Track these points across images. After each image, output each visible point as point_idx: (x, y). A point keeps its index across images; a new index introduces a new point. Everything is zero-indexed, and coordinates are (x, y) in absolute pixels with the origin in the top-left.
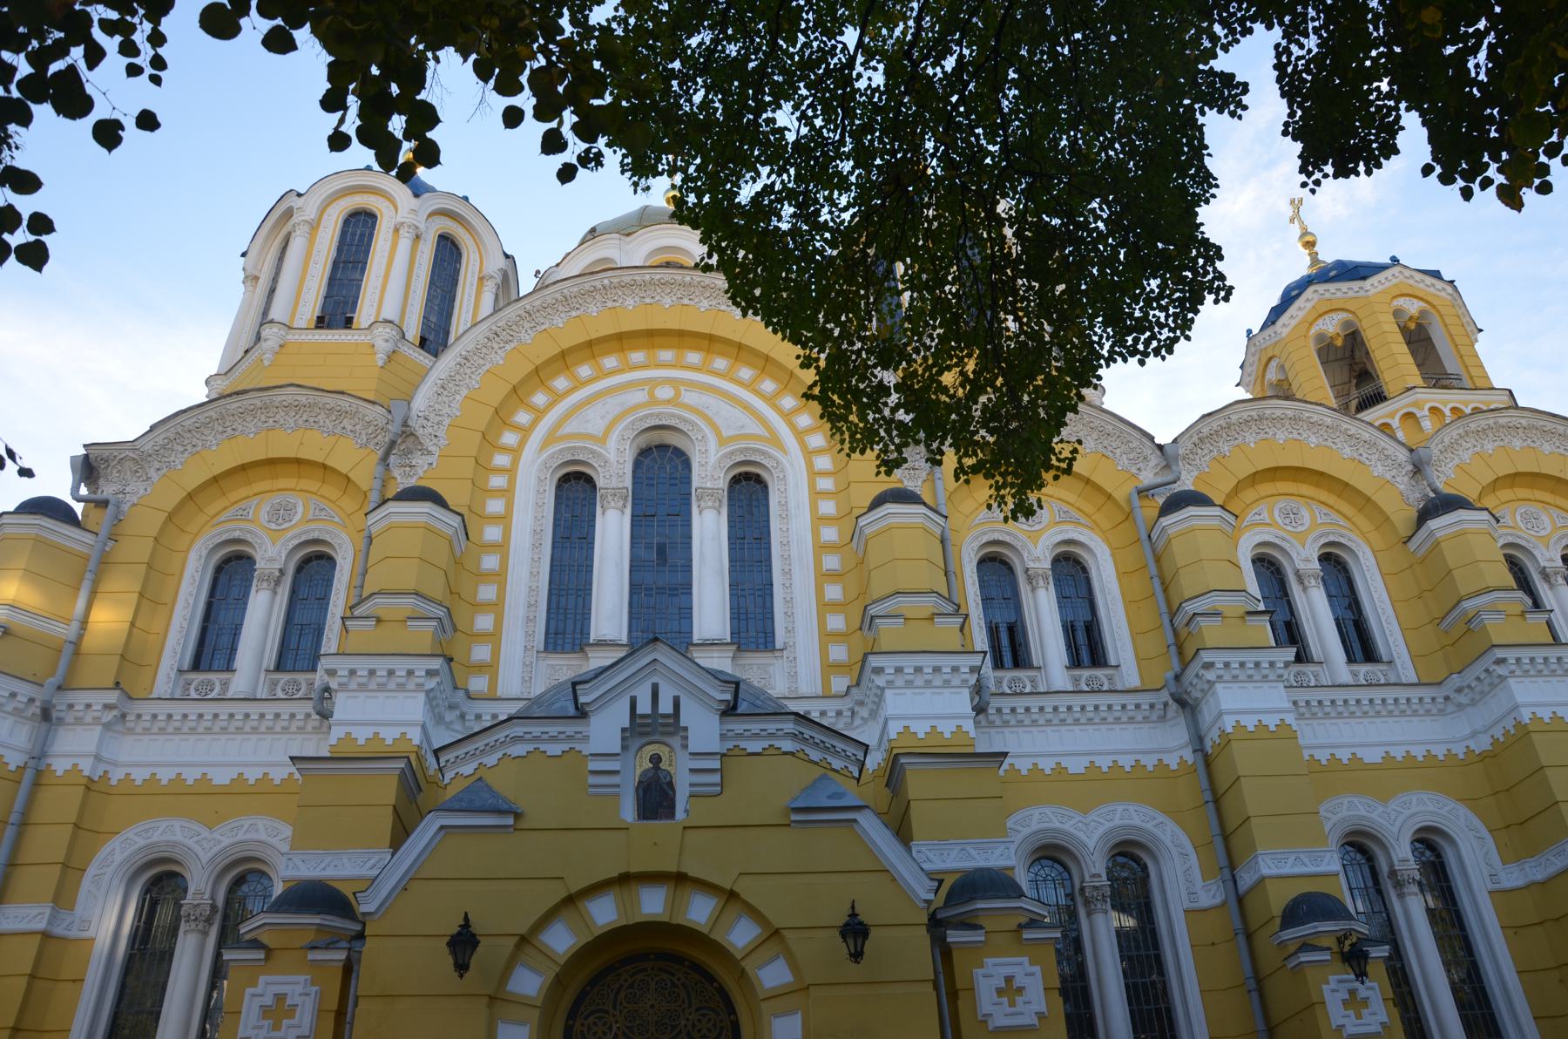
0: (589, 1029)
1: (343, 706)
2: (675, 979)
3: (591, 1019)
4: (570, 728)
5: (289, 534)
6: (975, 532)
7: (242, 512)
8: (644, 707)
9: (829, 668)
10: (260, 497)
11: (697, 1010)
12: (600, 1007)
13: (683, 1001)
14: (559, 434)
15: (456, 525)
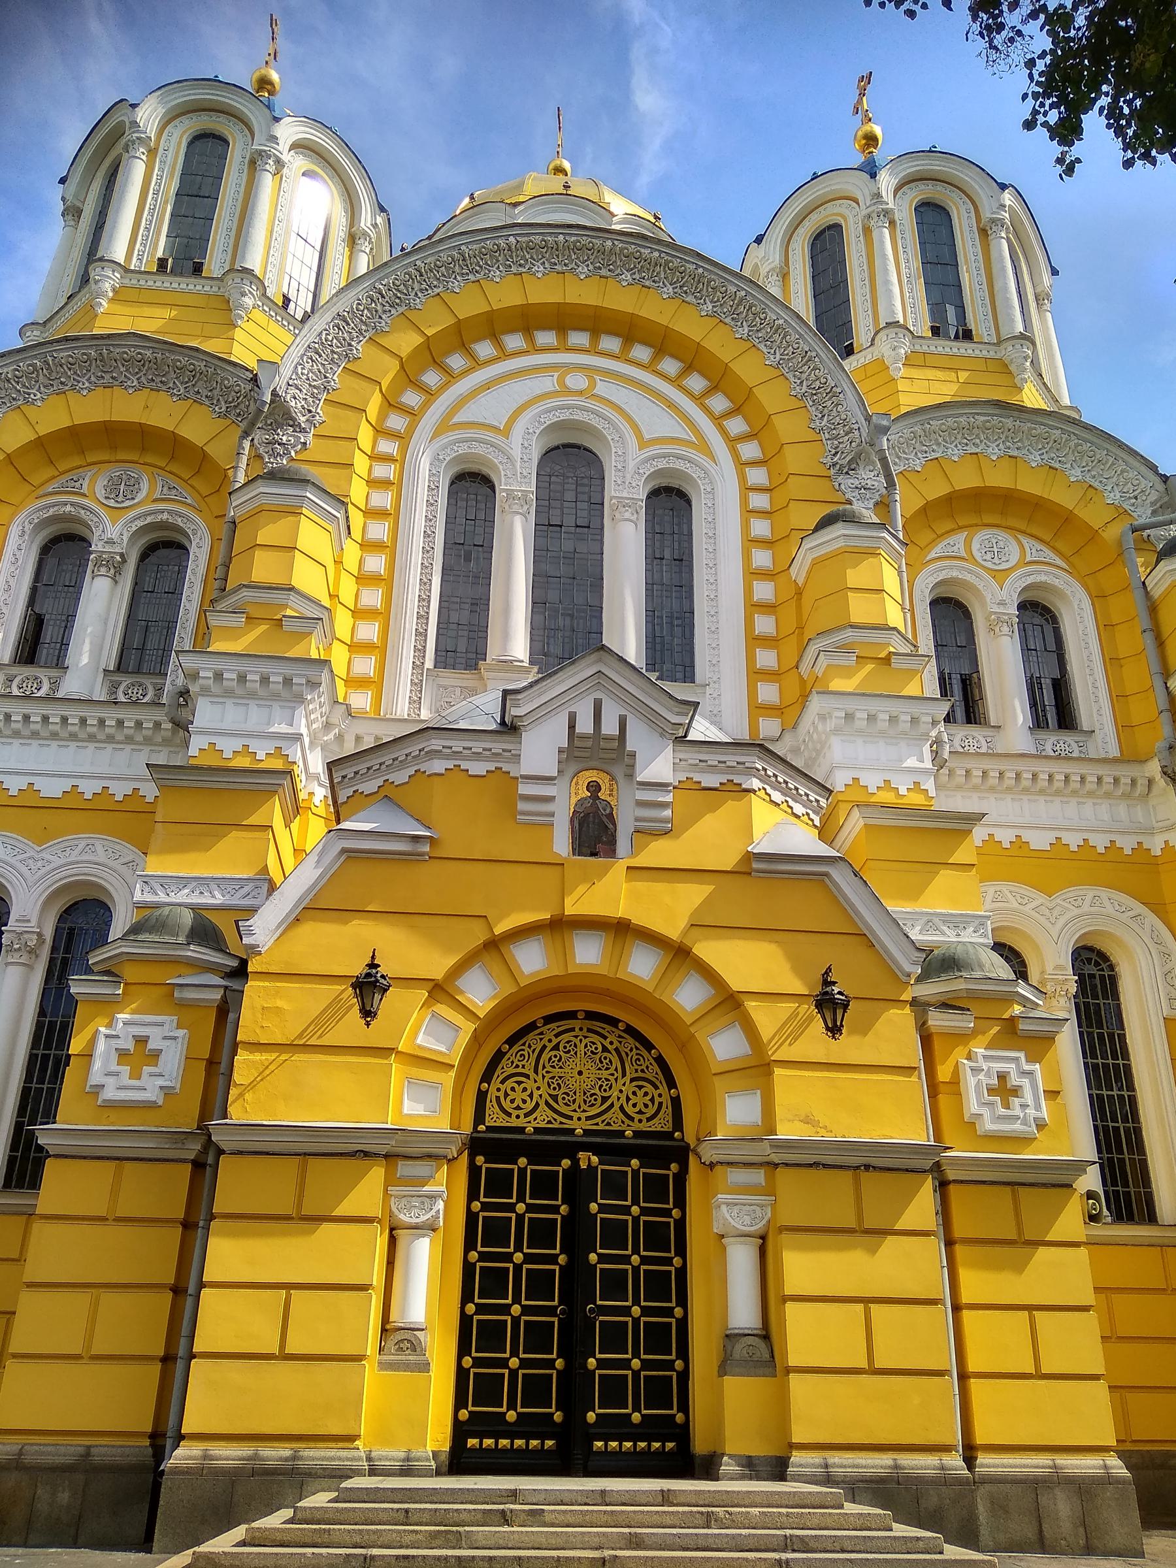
0: (506, 1095)
1: (205, 714)
2: (606, 1043)
3: (510, 1083)
4: (497, 746)
5: (132, 514)
6: (932, 567)
7: (73, 484)
8: (585, 726)
9: (757, 709)
10: (95, 468)
11: (632, 1080)
12: (520, 1070)
13: (616, 1070)
14: (455, 420)
15: (338, 515)
